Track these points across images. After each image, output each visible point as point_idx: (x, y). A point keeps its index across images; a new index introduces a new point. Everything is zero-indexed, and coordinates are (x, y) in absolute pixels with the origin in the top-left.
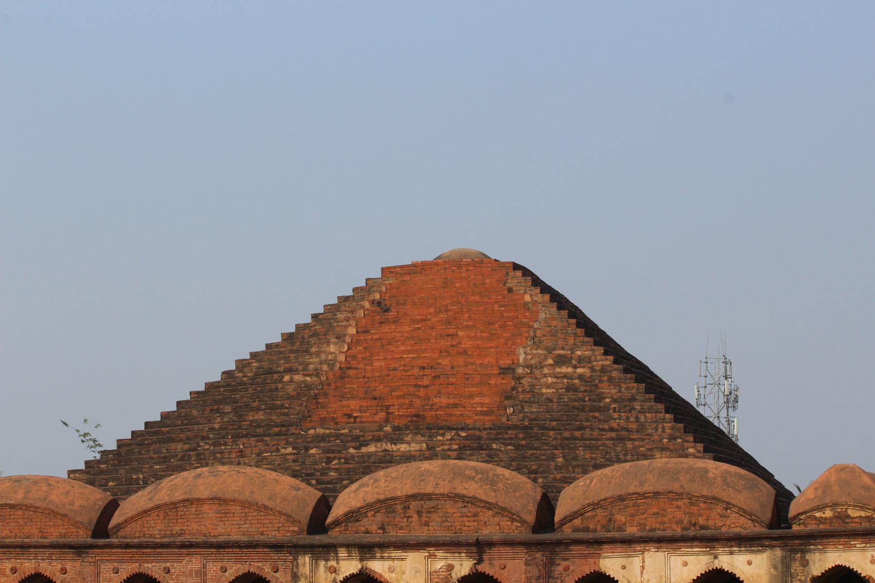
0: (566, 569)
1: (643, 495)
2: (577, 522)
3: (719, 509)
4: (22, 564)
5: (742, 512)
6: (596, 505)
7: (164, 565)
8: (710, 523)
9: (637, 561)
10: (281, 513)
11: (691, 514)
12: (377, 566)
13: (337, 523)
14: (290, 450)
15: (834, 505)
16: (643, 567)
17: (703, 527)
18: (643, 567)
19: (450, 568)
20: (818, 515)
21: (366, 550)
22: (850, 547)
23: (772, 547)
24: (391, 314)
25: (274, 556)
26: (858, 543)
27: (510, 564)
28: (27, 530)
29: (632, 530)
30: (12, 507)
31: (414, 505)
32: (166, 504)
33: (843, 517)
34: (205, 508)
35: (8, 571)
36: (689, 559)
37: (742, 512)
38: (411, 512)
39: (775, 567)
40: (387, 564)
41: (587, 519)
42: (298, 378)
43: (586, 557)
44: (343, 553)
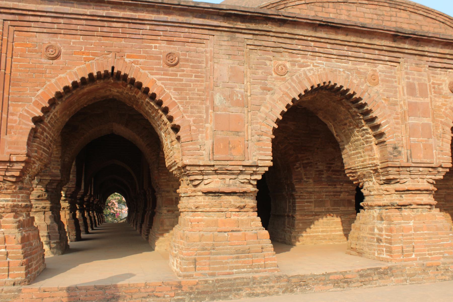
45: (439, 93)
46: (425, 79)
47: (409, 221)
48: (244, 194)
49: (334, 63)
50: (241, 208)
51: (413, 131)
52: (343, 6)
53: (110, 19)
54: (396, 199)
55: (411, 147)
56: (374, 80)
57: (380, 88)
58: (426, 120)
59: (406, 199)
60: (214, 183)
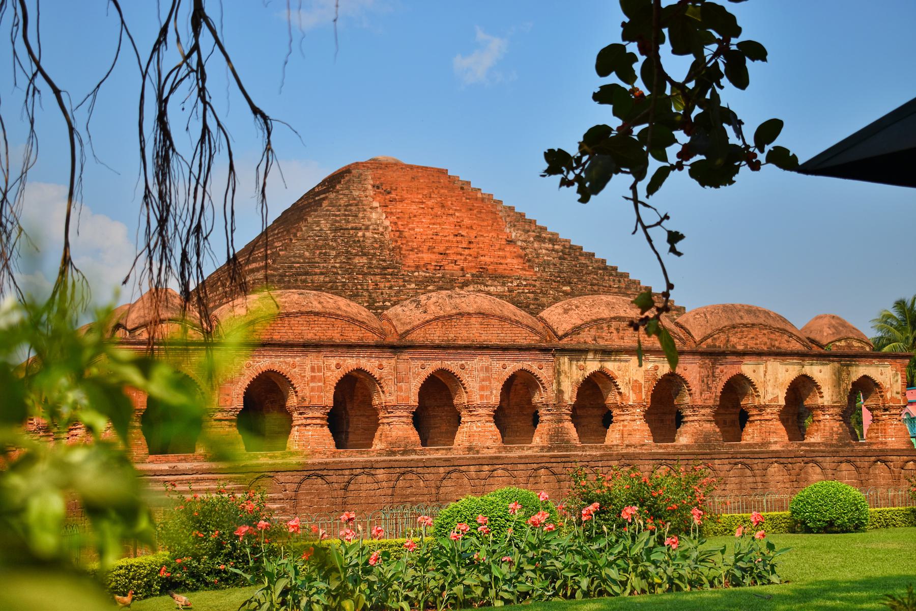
0: (722, 372)
1: (745, 325)
2: (709, 341)
3: (786, 337)
4: (345, 361)
5: (799, 339)
6: (721, 330)
7: (461, 363)
8: (782, 345)
9: (762, 368)
10: (528, 327)
11: (772, 339)
12: (611, 366)
13: (566, 335)
14: (413, 286)
15: (846, 339)
16: (766, 372)
17: (778, 348)
18: (766, 372)
19: (656, 368)
20: (838, 344)
21: (606, 353)
22: (871, 364)
23: (833, 361)
24: (393, 195)
25: (541, 357)
26: (875, 361)
27: (689, 367)
28: (329, 334)
29: (740, 348)
30: (317, 314)
31: (614, 324)
32: (444, 317)
33: (850, 346)
34: (473, 320)
35: (333, 367)
36: (790, 367)
37: (799, 339)
38: (612, 329)
39: (835, 374)
40: (617, 364)
41: (715, 339)
42: (368, 234)
43: (734, 363)
44: (590, 356)
45: (329, 369)
46: (321, 363)
47: (309, 432)
48: (231, 420)
49: (273, 359)
50: (230, 426)
51: (312, 389)
52: (286, 319)
53: (175, 349)
54: (304, 422)
55: (311, 397)
56: (294, 366)
57: (296, 370)
58: (320, 384)
59: (309, 421)
60: (219, 415)
